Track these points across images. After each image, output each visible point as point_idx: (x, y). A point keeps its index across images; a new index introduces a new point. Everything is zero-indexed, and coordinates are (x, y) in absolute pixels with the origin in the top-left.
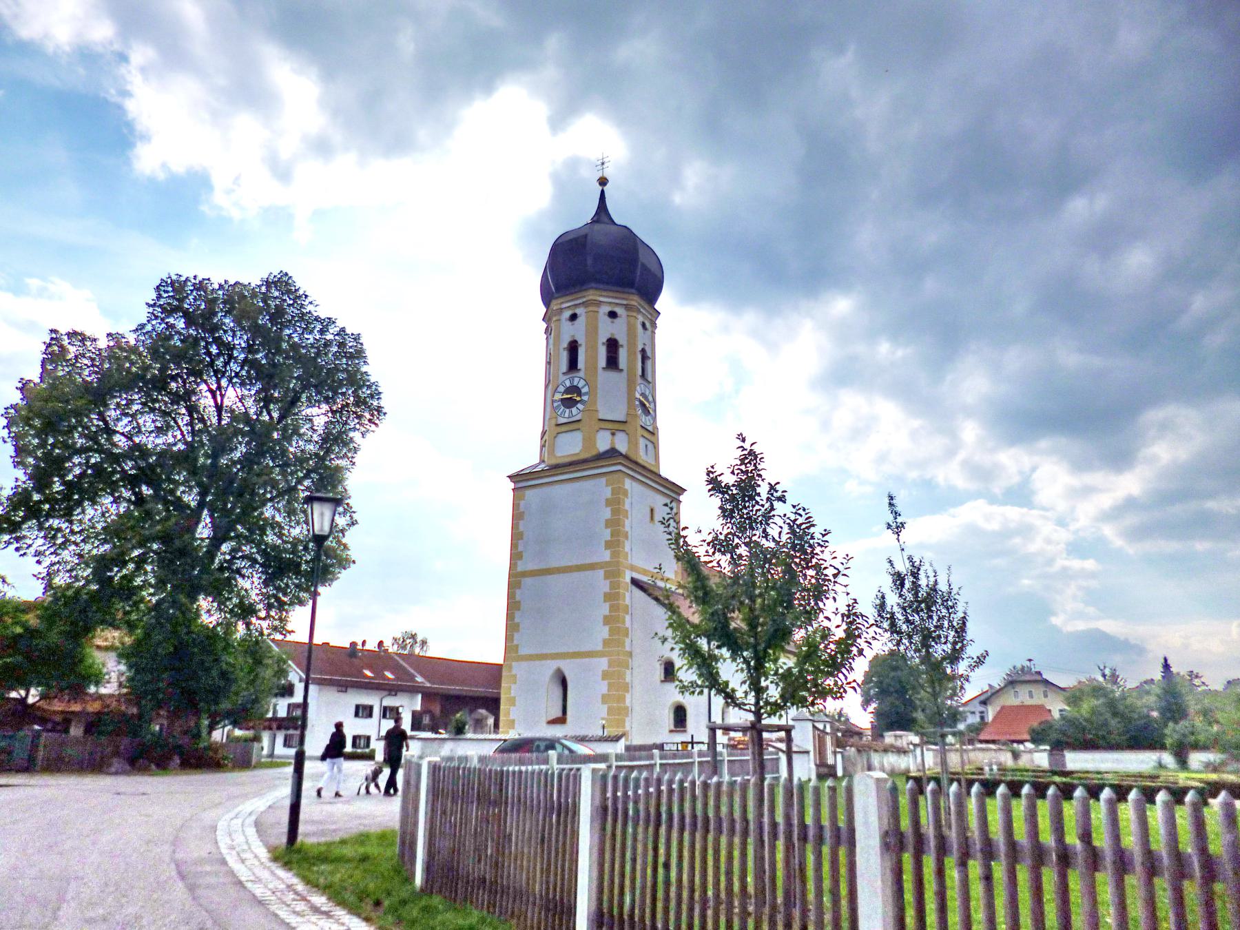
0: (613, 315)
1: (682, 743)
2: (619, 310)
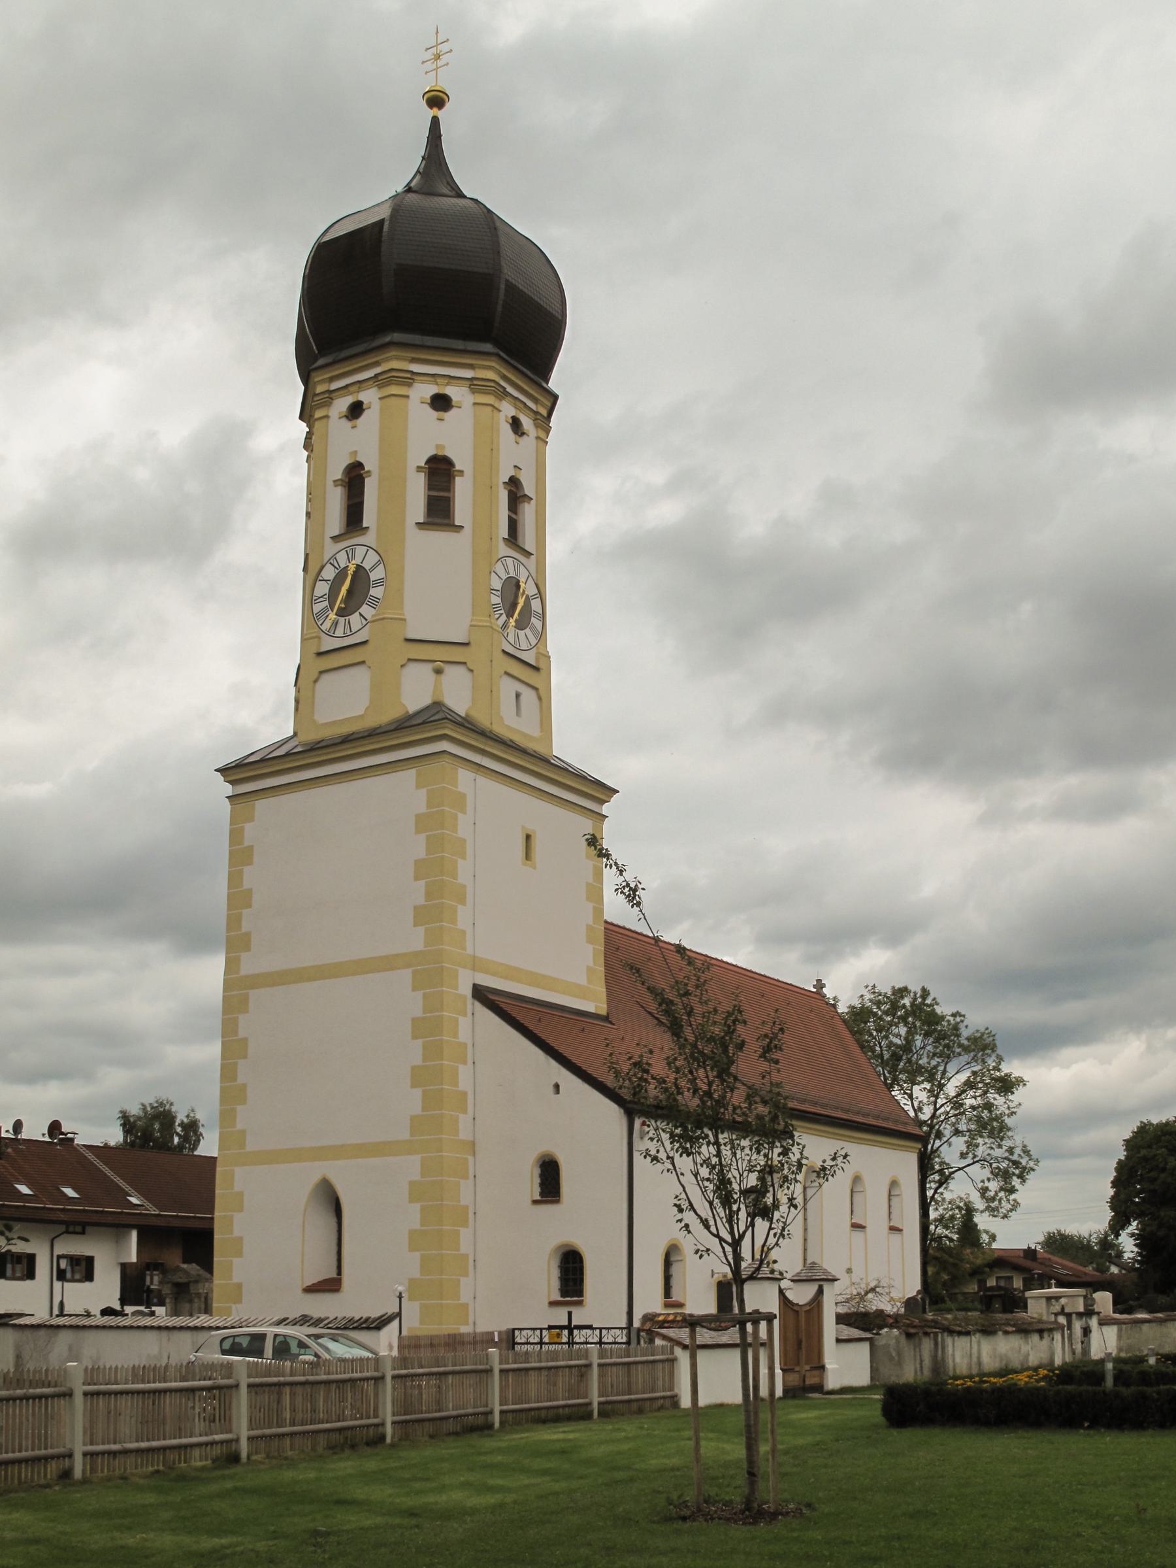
0: (516, 424)
1: (550, 1328)
2: (527, 422)
